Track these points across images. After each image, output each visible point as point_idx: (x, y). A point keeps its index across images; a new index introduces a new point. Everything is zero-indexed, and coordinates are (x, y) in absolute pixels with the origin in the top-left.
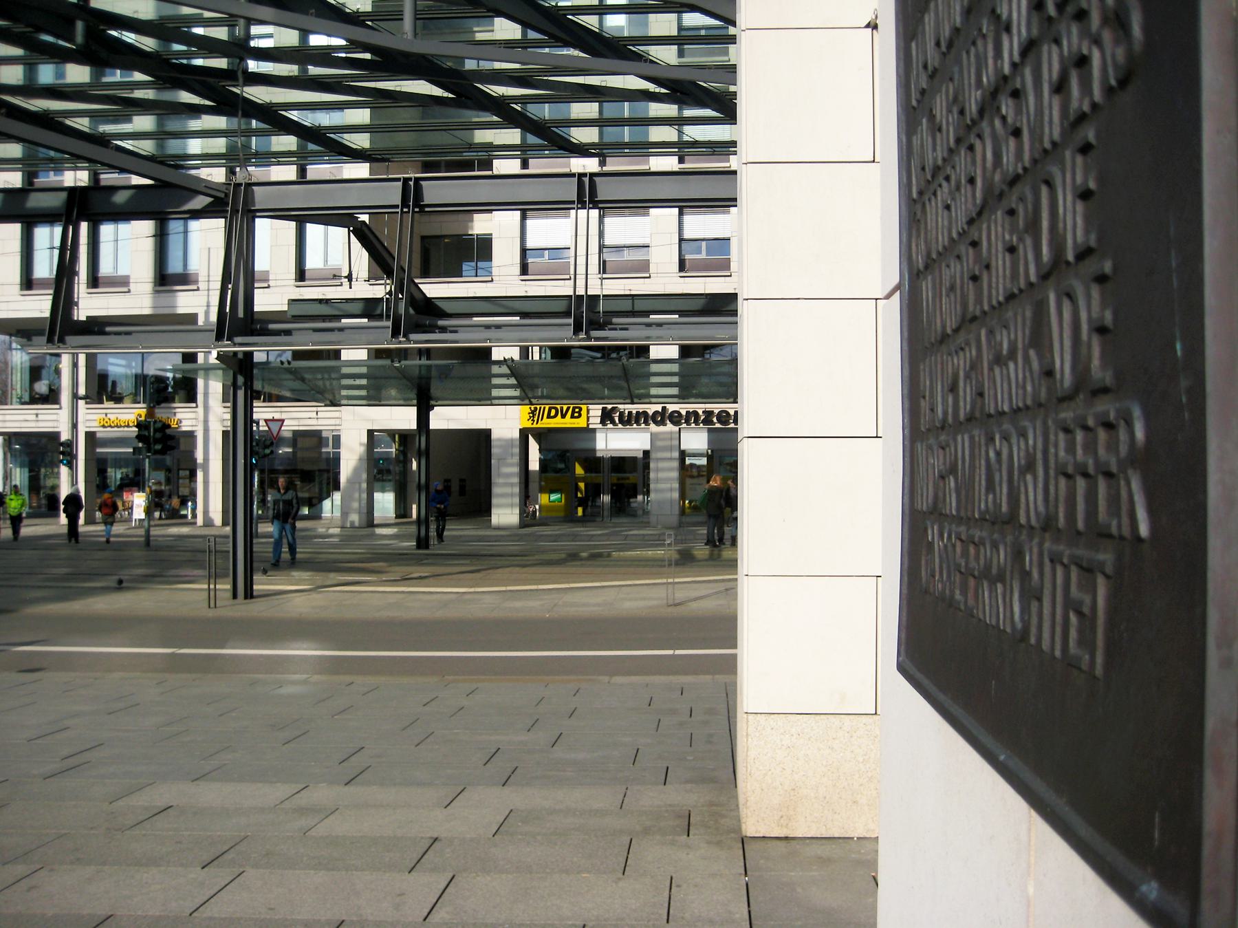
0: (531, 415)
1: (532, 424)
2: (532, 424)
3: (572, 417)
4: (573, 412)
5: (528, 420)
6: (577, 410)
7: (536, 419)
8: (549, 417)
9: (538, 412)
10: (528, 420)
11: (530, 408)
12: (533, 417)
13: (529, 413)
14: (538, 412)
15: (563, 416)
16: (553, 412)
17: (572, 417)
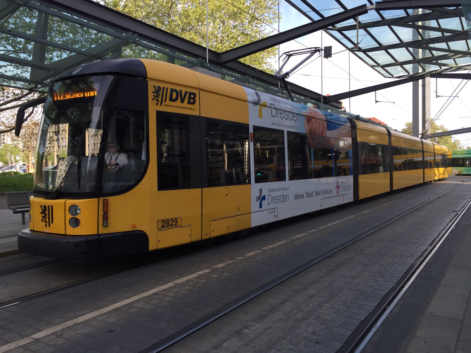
0: (156, 95)
1: (157, 104)
2: (157, 104)
3: (189, 103)
4: (190, 98)
5: (153, 99)
6: (192, 96)
7: (160, 99)
8: (171, 100)
9: (161, 92)
10: (153, 99)
11: (154, 86)
12: (158, 96)
13: (153, 92)
14: (161, 92)
15: (182, 101)
16: (174, 97)
17: (189, 103)
